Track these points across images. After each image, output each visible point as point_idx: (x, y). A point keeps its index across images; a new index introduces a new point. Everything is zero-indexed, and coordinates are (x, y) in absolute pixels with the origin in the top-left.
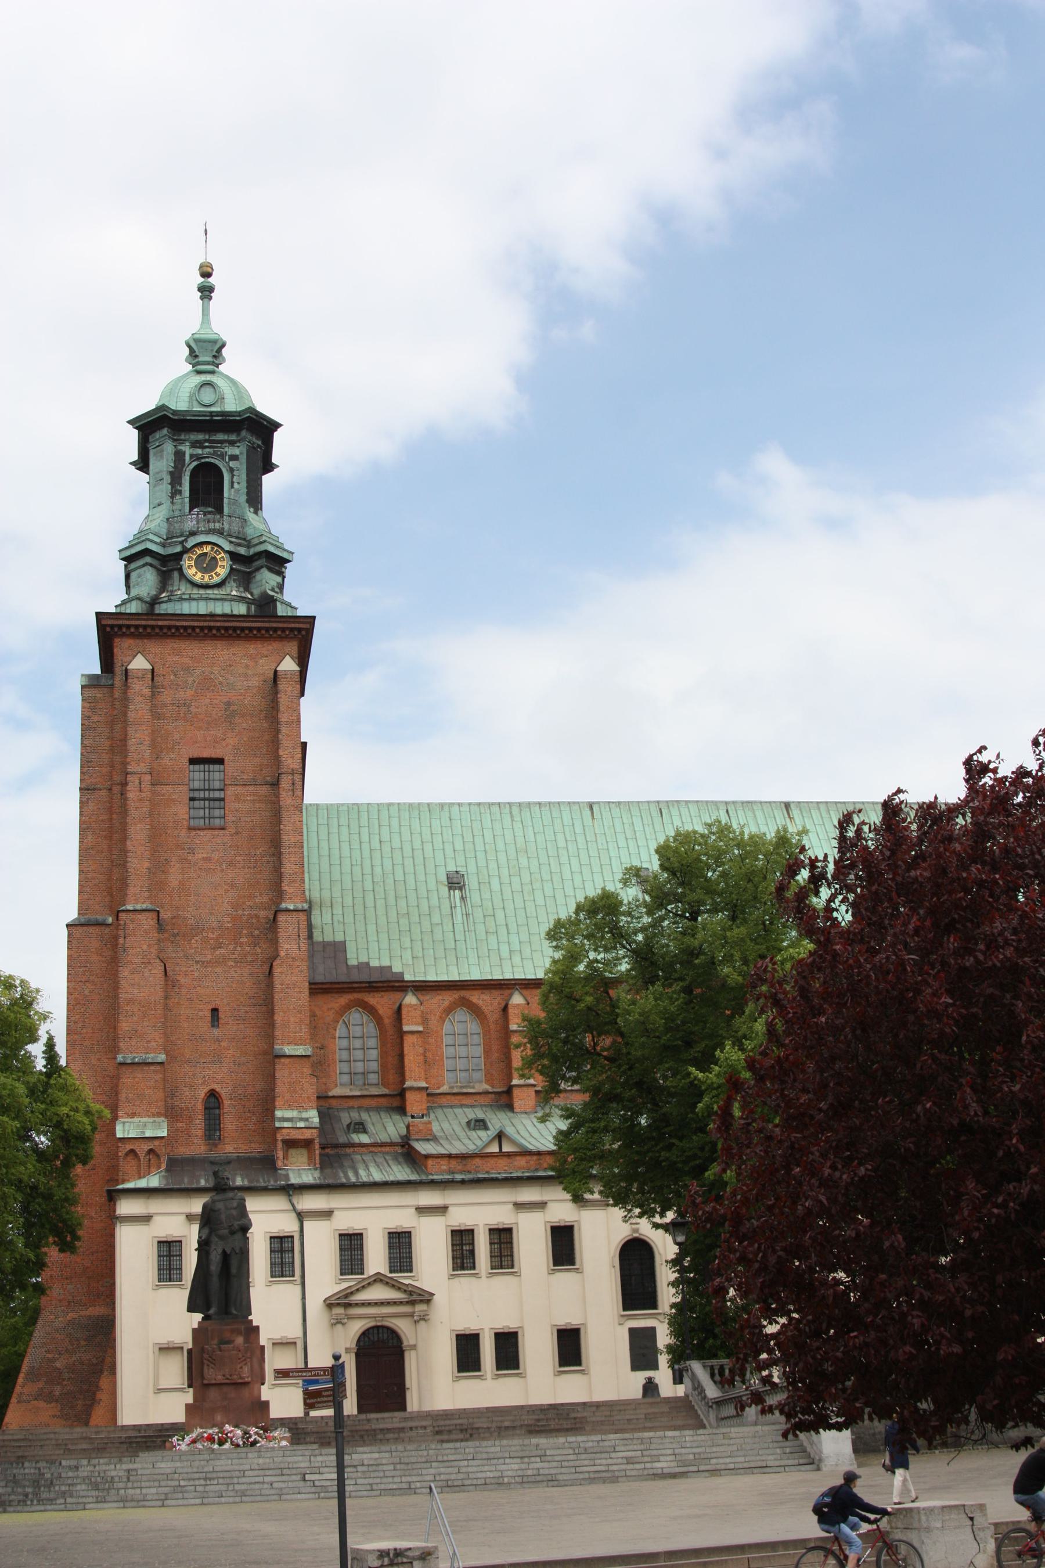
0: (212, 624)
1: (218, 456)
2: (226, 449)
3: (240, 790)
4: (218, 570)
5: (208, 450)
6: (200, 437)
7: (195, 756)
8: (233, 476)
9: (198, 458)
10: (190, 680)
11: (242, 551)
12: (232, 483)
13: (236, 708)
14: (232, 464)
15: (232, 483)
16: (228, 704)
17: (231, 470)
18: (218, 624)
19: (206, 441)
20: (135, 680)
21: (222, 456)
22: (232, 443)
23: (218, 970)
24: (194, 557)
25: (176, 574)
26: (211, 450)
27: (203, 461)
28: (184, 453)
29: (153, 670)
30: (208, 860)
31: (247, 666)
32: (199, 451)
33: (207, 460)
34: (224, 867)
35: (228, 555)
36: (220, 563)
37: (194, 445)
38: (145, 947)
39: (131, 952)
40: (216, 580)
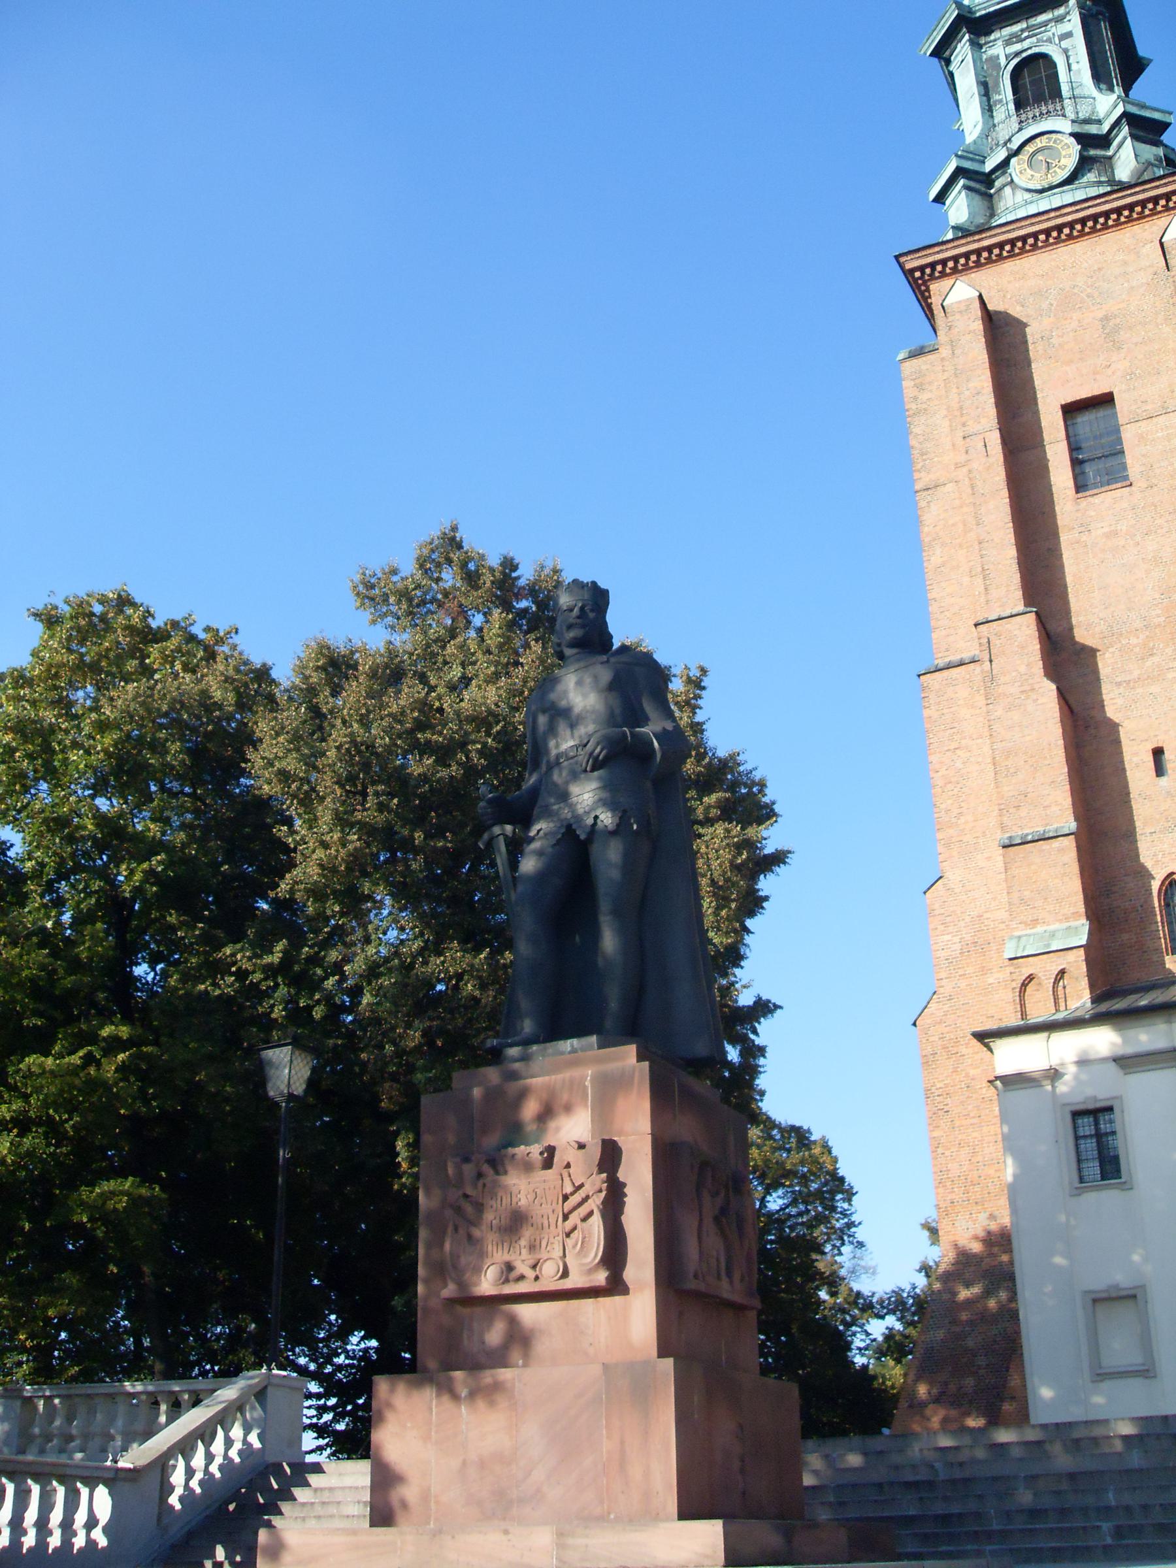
0: (1059, 221)
1: (1046, 41)
2: (1054, 29)
3: (1144, 426)
4: (1063, 161)
5: (1028, 41)
6: (1016, 28)
7: (1070, 399)
8: (1068, 58)
9: (1017, 54)
10: (1045, 305)
11: (1093, 129)
12: (1069, 65)
13: (1118, 321)
14: (1064, 44)
15: (1069, 65)
16: (1106, 318)
17: (1066, 51)
18: (1069, 218)
19: (1022, 31)
20: (957, 316)
21: (1049, 40)
22: (1059, 20)
23: (1155, 689)
24: (1026, 158)
25: (1008, 190)
26: (1034, 39)
27: (1024, 55)
28: (998, 57)
29: (980, 297)
30: (1114, 534)
31: (1125, 263)
32: (1017, 47)
33: (1029, 52)
34: (1138, 538)
35: (1072, 140)
36: (1063, 153)
37: (1008, 42)
38: (1022, 669)
39: (1003, 679)
40: (1063, 174)
